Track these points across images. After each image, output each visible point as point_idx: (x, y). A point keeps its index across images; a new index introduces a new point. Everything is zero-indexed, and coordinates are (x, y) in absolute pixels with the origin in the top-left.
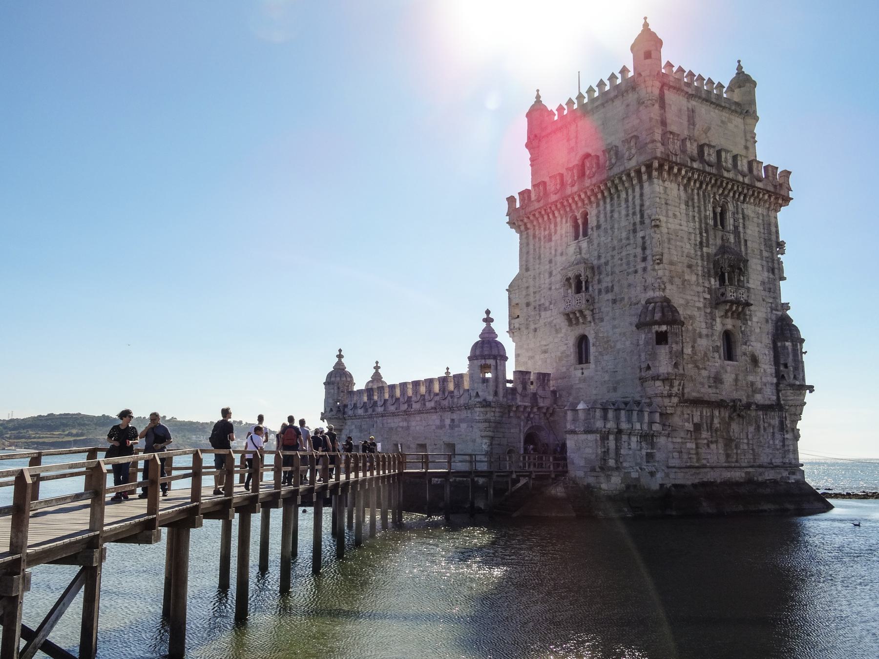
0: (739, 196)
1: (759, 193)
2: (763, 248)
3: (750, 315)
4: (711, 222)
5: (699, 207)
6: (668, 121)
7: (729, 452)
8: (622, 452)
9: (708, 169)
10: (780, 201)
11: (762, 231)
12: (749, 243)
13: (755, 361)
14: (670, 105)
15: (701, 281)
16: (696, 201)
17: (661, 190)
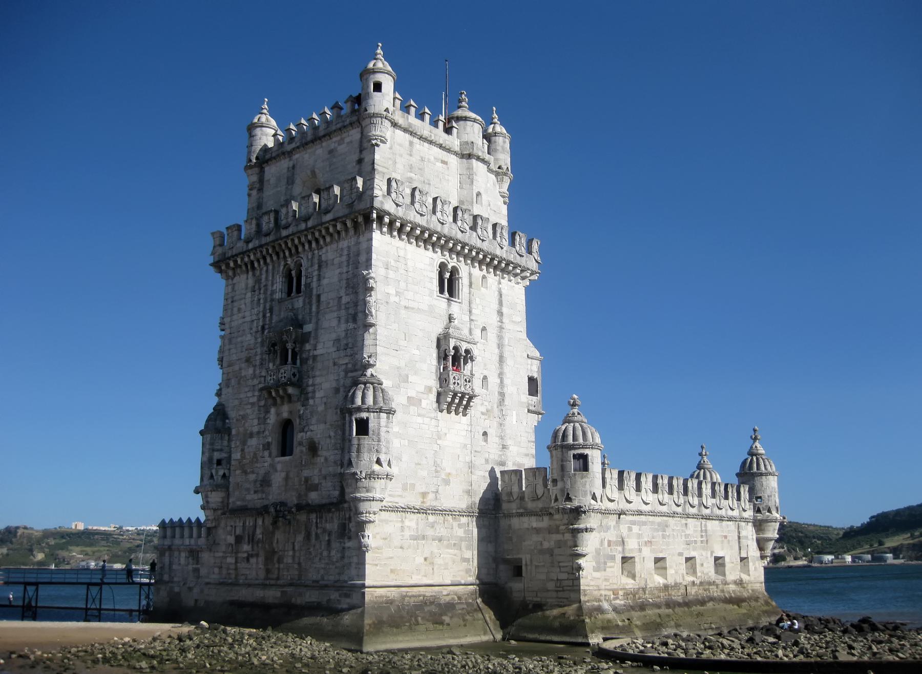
0: (310, 243)
2: (342, 293)
3: (314, 392)
5: (266, 286)
6: (265, 200)
7: (270, 567)
8: (174, 567)
11: (345, 270)
13: (313, 448)
14: (269, 180)
16: (263, 280)
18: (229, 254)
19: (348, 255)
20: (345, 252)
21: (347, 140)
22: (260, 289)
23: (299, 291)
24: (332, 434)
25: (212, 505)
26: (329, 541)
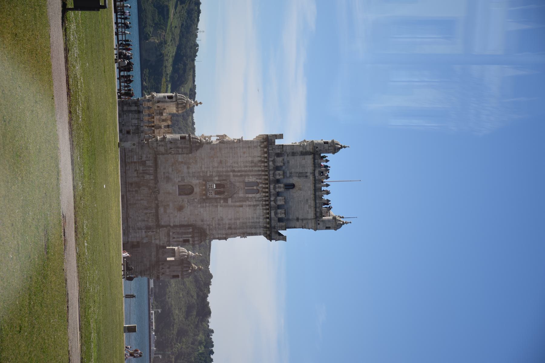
0: (266, 201)
1: (268, 213)
2: (241, 220)
3: (203, 207)
4: (247, 180)
5: (252, 171)
6: (295, 157)
8: (130, 114)
9: (271, 172)
10: (268, 232)
11: (250, 221)
12: (241, 208)
13: (181, 208)
14: (304, 159)
15: (215, 170)
17: (255, 144)
18: (270, 148)
19: (256, 222)
20: (258, 221)
21: (310, 210)
22: (252, 167)
23: (247, 192)
24: (186, 219)
25: (158, 148)
26: (144, 221)
